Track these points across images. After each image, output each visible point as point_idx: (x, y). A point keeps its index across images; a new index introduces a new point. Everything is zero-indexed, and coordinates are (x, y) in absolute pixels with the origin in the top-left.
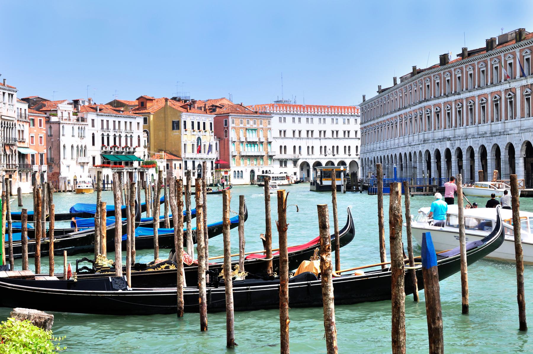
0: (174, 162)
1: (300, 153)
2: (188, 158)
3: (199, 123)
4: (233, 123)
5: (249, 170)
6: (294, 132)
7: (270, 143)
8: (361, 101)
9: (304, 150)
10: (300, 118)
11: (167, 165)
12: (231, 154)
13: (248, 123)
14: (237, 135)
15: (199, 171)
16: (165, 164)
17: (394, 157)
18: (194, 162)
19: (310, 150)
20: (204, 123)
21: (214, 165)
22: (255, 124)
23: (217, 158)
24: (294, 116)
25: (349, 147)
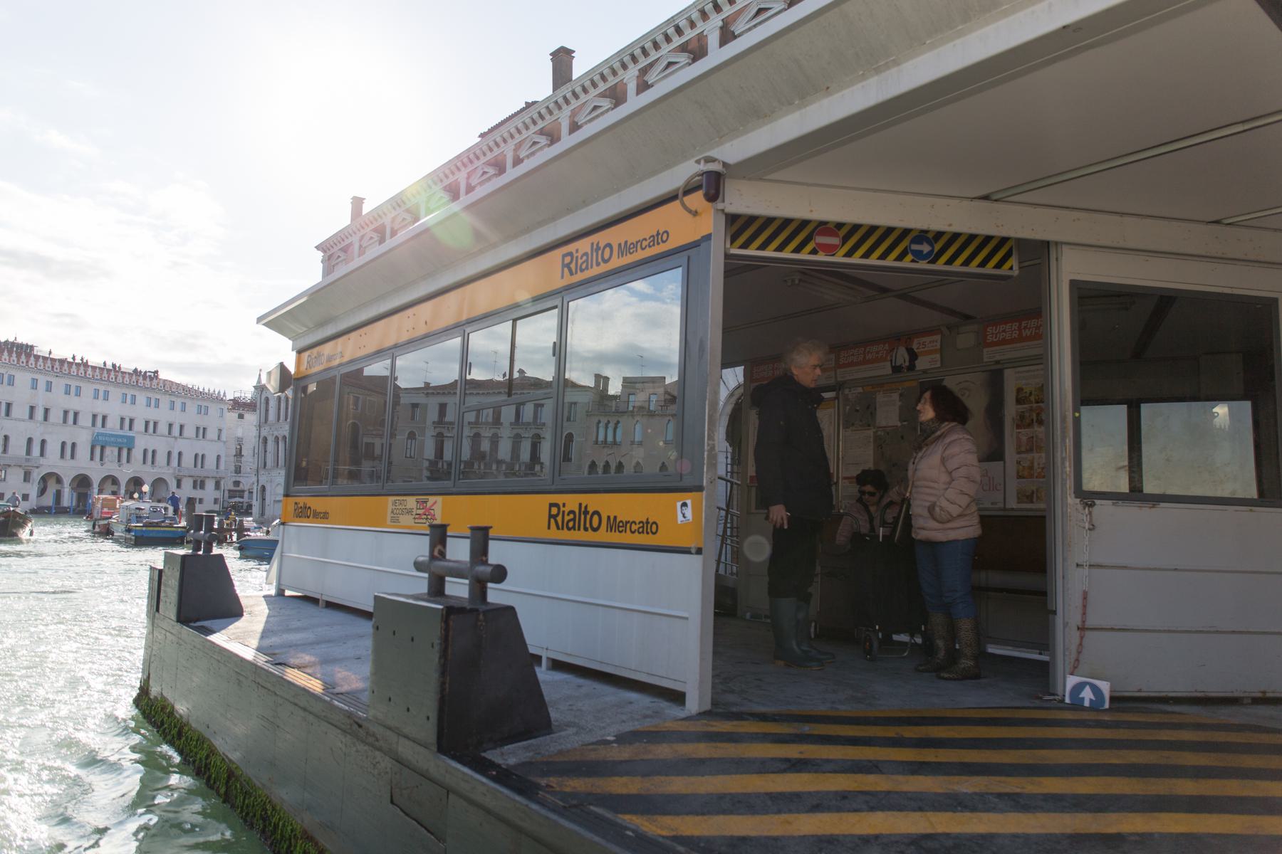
1: (42, 454)
6: (32, 408)
9: (53, 448)
19: (67, 450)
24: (36, 376)
25: (154, 452)
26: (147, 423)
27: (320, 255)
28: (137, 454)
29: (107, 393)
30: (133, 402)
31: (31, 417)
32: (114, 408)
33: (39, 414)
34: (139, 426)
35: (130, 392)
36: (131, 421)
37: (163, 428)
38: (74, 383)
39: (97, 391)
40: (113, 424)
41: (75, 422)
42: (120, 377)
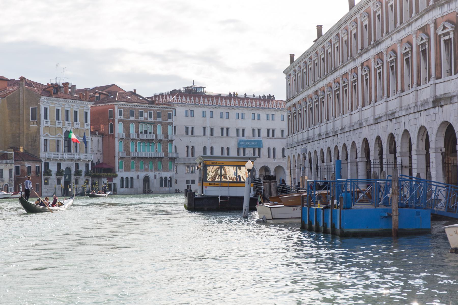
0: (27, 164)
2: (49, 159)
3: (67, 111)
4: (120, 114)
5: (142, 175)
6: (204, 129)
7: (172, 141)
8: (288, 64)
10: (212, 113)
11: (17, 168)
12: (117, 154)
13: (141, 115)
14: (126, 130)
15: (67, 177)
16: (13, 167)
17: (349, 148)
18: (59, 165)
20: (76, 112)
21: (90, 169)
22: (150, 116)
23: (99, 160)
25: (274, 149)
26: (268, 131)
27: (285, 76)
28: (264, 151)
29: (243, 114)
30: (259, 119)
31: (204, 134)
32: (248, 124)
33: (208, 132)
34: (264, 133)
35: (256, 112)
36: (259, 130)
37: (278, 133)
38: (225, 111)
39: (238, 114)
40: (248, 133)
41: (227, 135)
42: (250, 104)
